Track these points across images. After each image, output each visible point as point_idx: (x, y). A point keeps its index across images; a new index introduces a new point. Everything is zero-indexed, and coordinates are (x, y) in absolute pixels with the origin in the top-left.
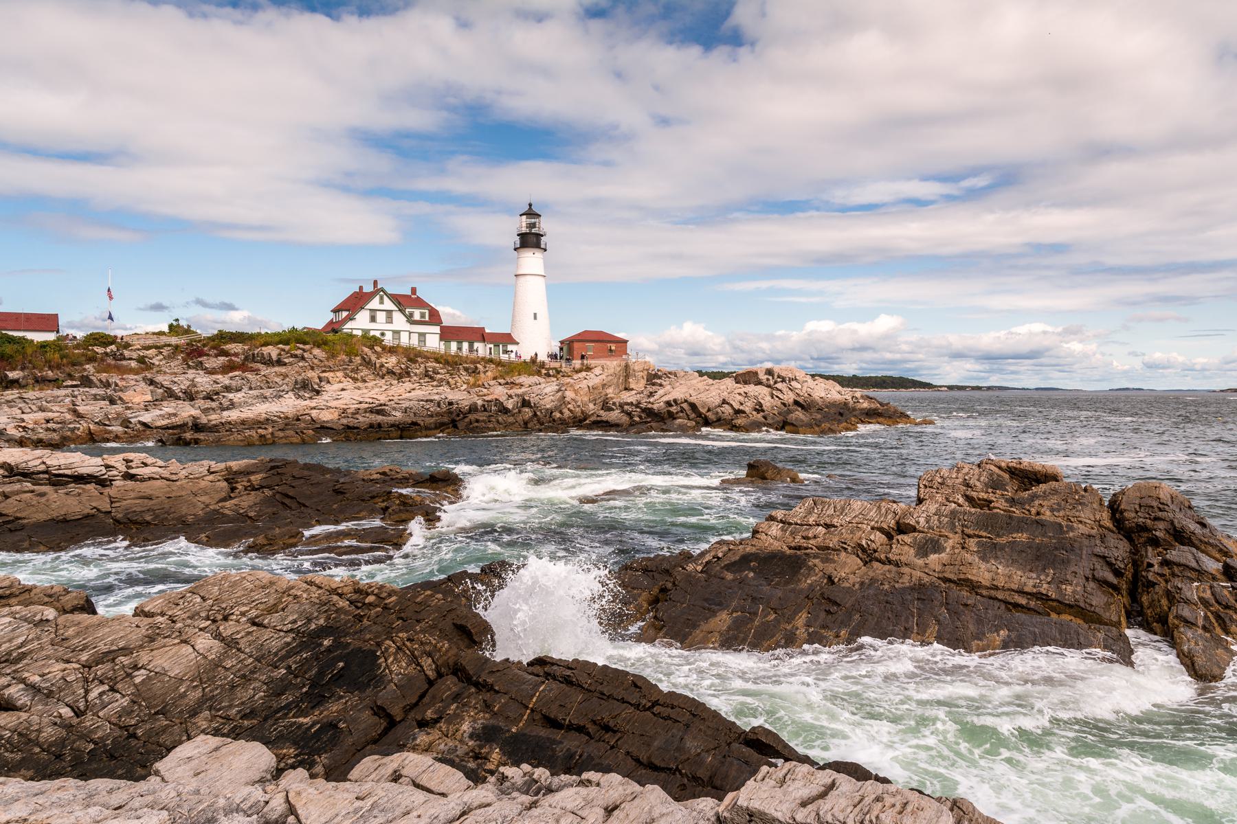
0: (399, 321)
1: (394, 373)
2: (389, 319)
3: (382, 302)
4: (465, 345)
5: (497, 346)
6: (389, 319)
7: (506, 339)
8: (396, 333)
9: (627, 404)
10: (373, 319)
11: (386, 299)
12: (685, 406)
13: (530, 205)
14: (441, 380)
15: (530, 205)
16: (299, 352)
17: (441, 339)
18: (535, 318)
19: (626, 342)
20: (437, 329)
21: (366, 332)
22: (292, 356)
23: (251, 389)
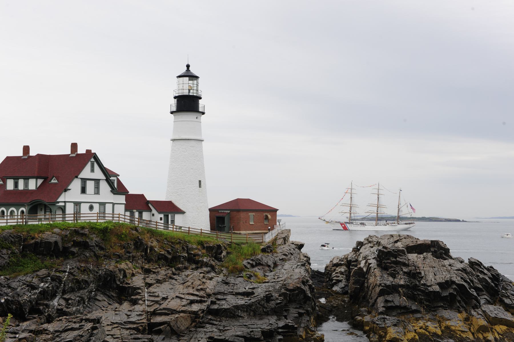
0: (106, 193)
1: (165, 258)
2: (97, 191)
3: (92, 170)
4: (137, 215)
5: (167, 217)
6: (97, 191)
7: (168, 208)
8: (103, 205)
9: (402, 286)
10: (83, 190)
11: (96, 165)
12: (455, 286)
13: (188, 66)
14: (206, 265)
15: (188, 66)
16: (80, 239)
17: (126, 210)
18: (200, 186)
19: (274, 211)
20: (122, 199)
21: (77, 204)
22: (76, 244)
23: (64, 292)
